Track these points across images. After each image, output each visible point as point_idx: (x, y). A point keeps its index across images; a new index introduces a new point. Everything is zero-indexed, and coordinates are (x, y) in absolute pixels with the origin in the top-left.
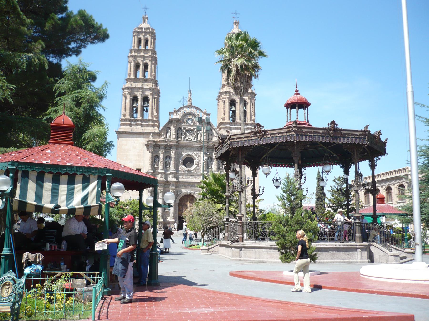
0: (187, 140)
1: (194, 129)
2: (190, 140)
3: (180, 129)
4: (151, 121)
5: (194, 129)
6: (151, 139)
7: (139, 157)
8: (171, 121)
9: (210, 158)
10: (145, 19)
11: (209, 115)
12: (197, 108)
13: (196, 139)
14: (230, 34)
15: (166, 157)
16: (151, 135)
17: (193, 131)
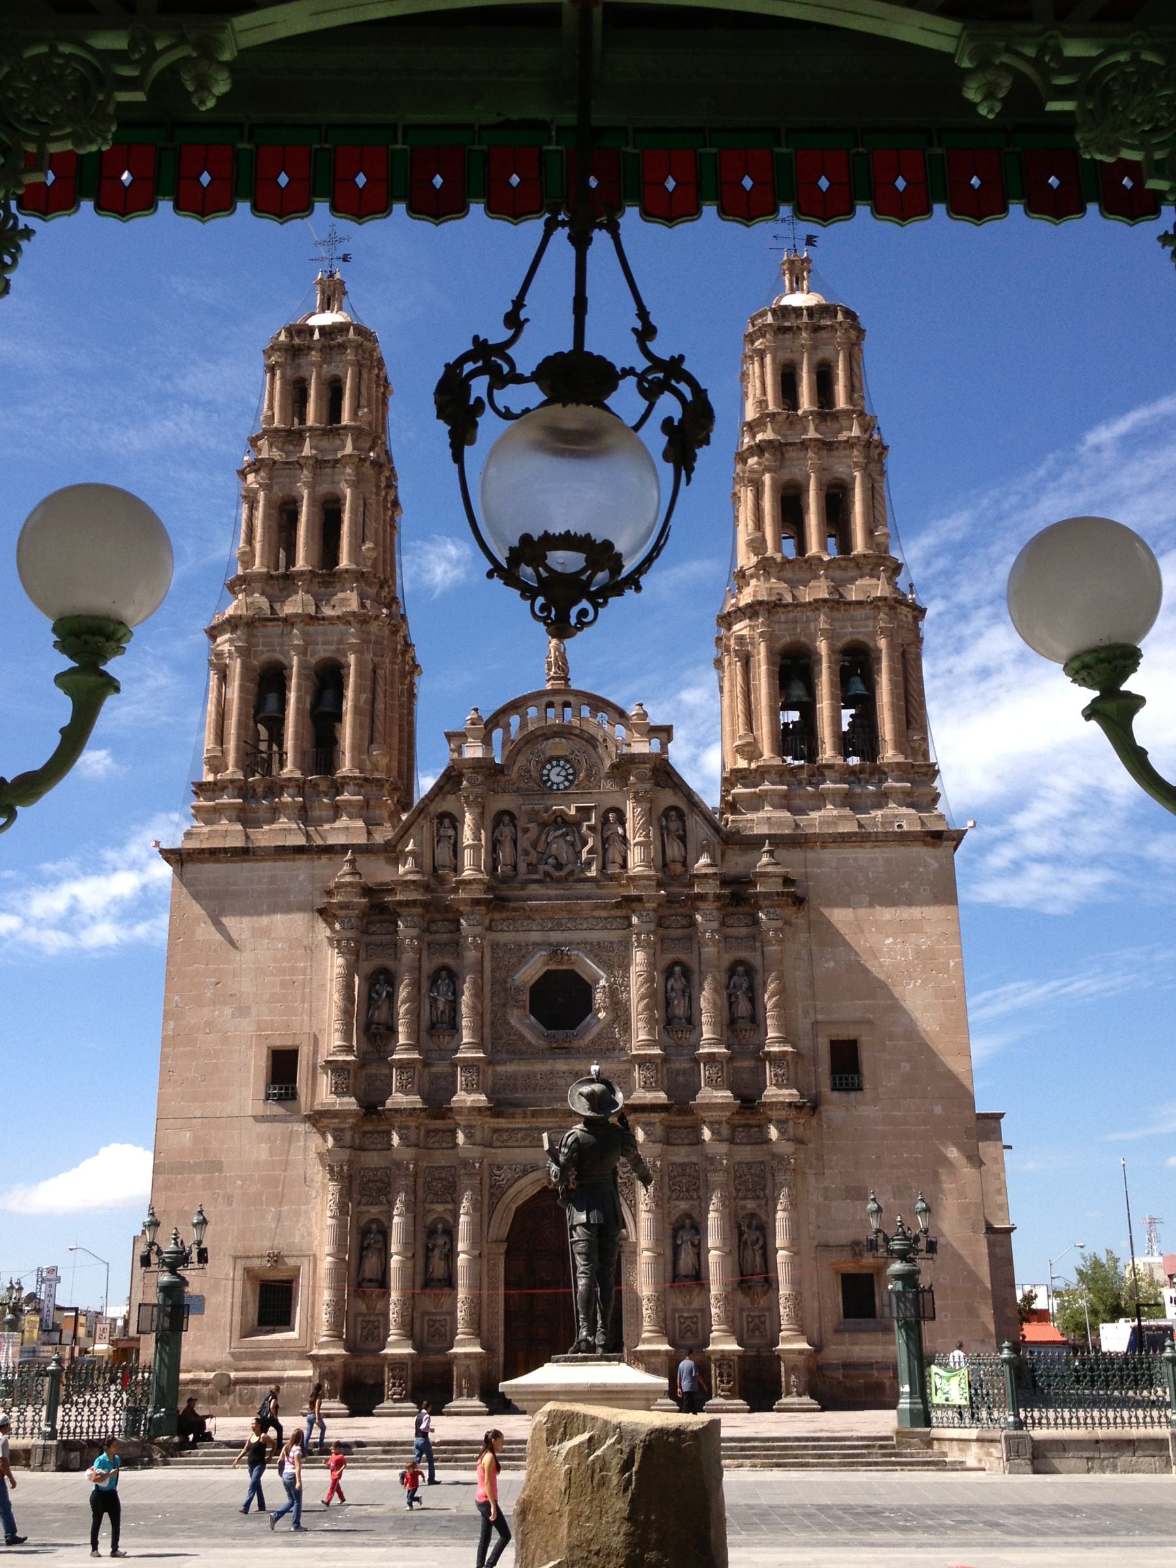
0: (547, 874)
1: (584, 812)
2: (562, 873)
3: (506, 819)
4: (351, 788)
5: (584, 812)
6: (348, 879)
7: (283, 984)
8: (450, 780)
9: (677, 969)
10: (331, 296)
11: (665, 732)
12: (599, 704)
13: (594, 868)
14: (762, 315)
15: (434, 979)
16: (349, 856)
17: (578, 825)
